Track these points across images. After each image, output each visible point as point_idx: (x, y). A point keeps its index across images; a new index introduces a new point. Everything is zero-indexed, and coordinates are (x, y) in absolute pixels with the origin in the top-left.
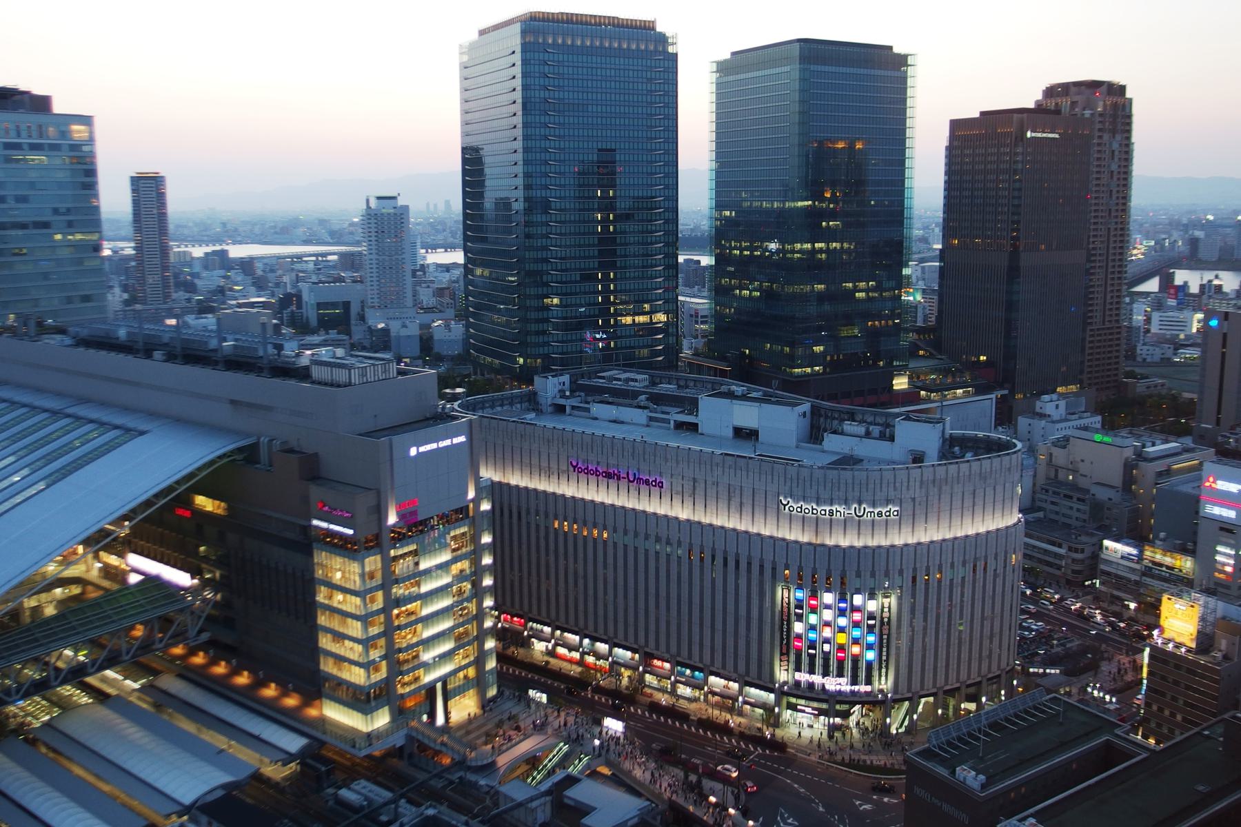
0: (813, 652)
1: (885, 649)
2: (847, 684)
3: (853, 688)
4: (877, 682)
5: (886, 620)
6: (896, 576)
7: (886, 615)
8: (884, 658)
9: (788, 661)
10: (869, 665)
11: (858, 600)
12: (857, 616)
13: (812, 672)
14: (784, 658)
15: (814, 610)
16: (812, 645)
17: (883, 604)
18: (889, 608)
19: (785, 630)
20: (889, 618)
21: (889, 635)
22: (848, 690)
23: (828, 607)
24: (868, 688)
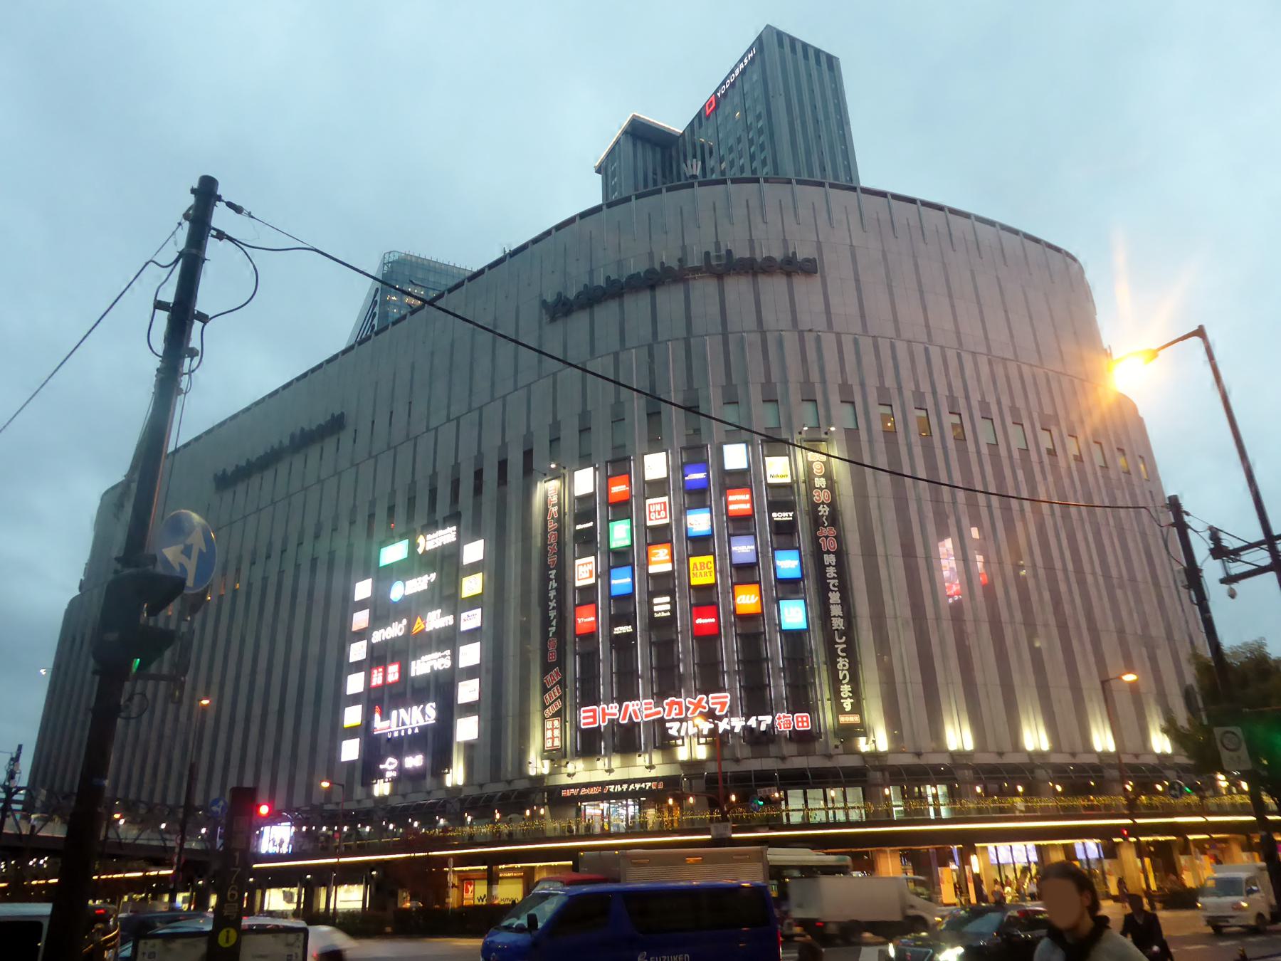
1: (834, 597)
3: (752, 722)
4: (828, 704)
5: (824, 510)
6: (835, 398)
7: (822, 496)
8: (838, 623)
9: (562, 684)
13: (626, 693)
14: (554, 676)
15: (621, 509)
16: (622, 608)
17: (809, 466)
18: (828, 476)
19: (552, 594)
20: (832, 505)
21: (840, 554)
23: (658, 487)
24: (802, 722)
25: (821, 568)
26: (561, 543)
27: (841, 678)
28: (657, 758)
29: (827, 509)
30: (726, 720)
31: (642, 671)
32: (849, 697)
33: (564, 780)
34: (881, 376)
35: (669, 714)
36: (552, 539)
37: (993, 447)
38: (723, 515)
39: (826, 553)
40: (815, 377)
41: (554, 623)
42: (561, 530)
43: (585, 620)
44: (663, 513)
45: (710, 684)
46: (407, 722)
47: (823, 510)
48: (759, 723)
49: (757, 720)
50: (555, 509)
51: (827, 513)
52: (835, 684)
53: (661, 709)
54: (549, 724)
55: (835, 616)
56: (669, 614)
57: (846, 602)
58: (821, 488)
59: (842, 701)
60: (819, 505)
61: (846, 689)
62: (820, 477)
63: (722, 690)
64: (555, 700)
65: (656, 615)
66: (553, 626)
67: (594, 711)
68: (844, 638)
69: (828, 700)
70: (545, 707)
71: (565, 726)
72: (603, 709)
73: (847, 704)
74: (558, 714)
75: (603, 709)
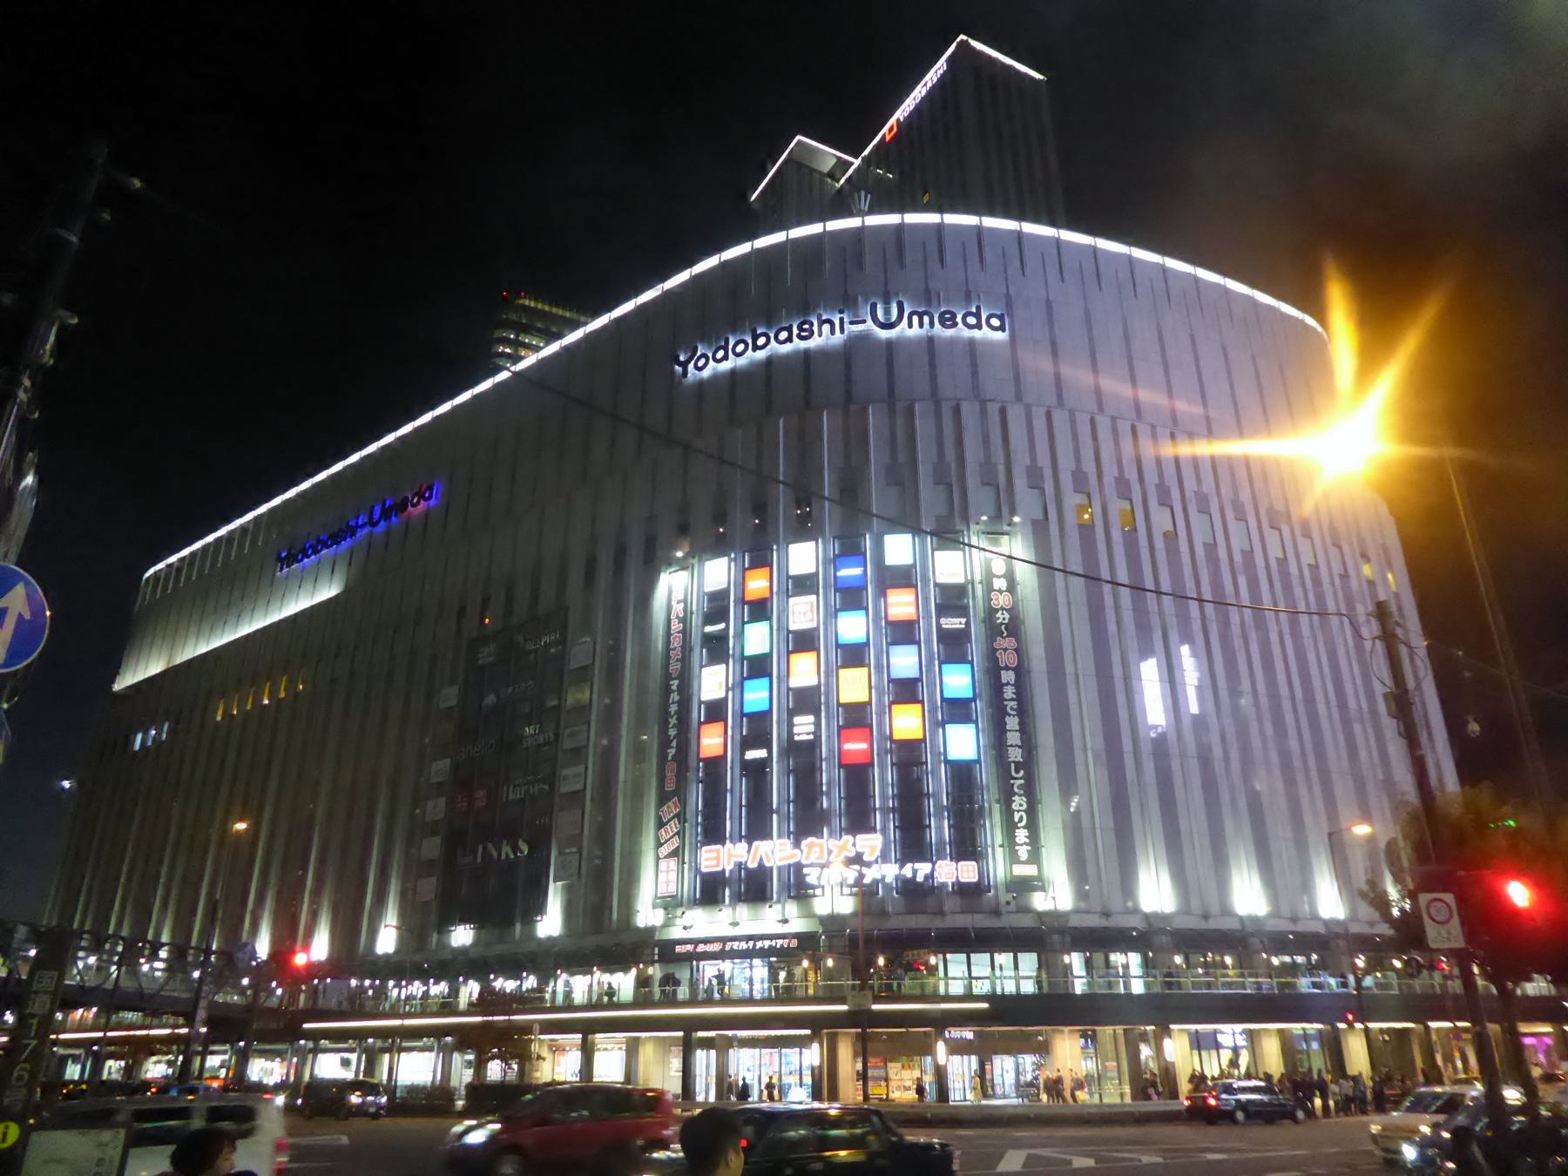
0: (761, 753)
1: (1012, 723)
2: (884, 857)
3: (908, 871)
4: (999, 852)
7: (1002, 600)
8: (1015, 755)
10: (962, 774)
11: (899, 548)
12: (901, 604)
13: (757, 830)
14: (671, 808)
15: (760, 609)
16: (757, 729)
19: (673, 708)
21: (1021, 671)
22: (890, 879)
23: (804, 585)
24: (968, 872)
25: (997, 687)
26: (687, 648)
27: (1016, 820)
28: (792, 909)
29: (1007, 616)
30: (875, 867)
31: (779, 804)
32: (1025, 843)
33: (676, 933)
34: (1078, 459)
35: (807, 858)
36: (676, 643)
37: (1211, 548)
38: (881, 619)
39: (1003, 669)
40: (999, 457)
41: (674, 744)
42: (685, 633)
43: (711, 741)
44: (809, 614)
45: (859, 821)
46: (495, 854)
47: (1002, 617)
48: (915, 872)
49: (913, 867)
50: (682, 605)
51: (1006, 621)
52: (1010, 827)
53: (797, 851)
54: (663, 864)
55: (1012, 746)
56: (811, 737)
57: (1026, 730)
58: (1000, 591)
59: (1017, 848)
60: (997, 611)
61: (1022, 835)
62: (999, 577)
63: (873, 830)
64: (672, 837)
65: (796, 738)
66: (672, 747)
67: (718, 851)
68: (1022, 773)
69: (1000, 846)
70: (659, 845)
71: (683, 868)
72: (729, 850)
73: (1023, 852)
74: (674, 853)
75: (729, 850)
